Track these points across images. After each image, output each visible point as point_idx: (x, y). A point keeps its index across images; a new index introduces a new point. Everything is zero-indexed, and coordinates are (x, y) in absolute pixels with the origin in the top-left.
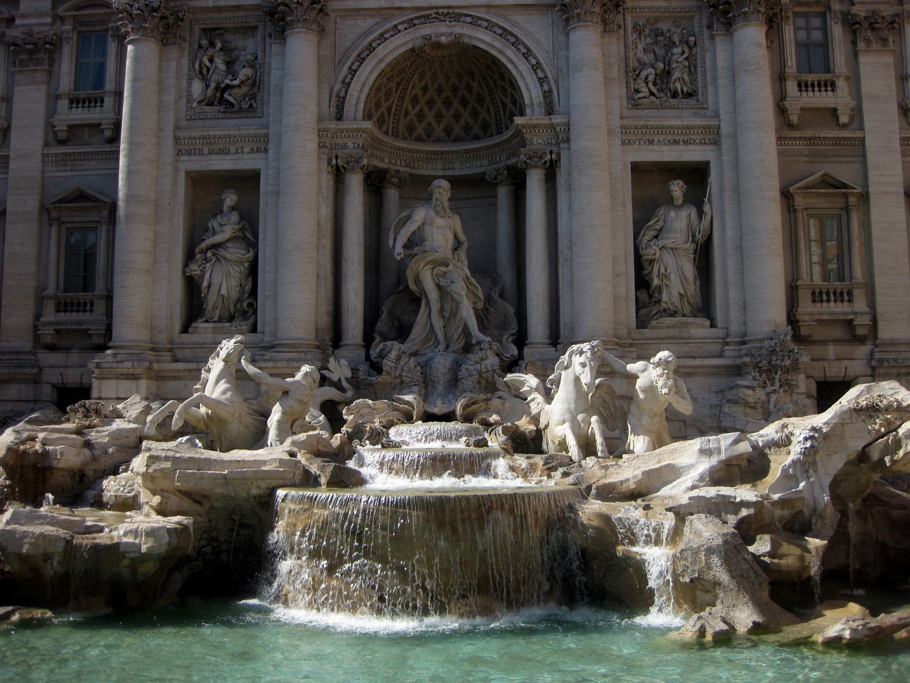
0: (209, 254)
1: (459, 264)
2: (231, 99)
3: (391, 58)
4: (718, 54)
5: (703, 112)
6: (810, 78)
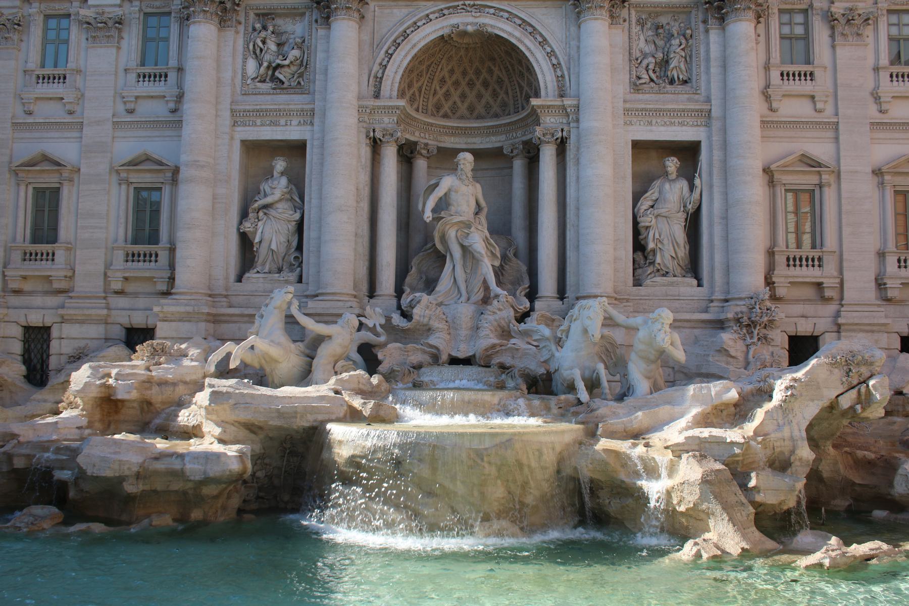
0: (261, 214)
1: (480, 227)
2: (281, 77)
3: (423, 44)
4: (711, 46)
5: (697, 96)
6: (791, 68)
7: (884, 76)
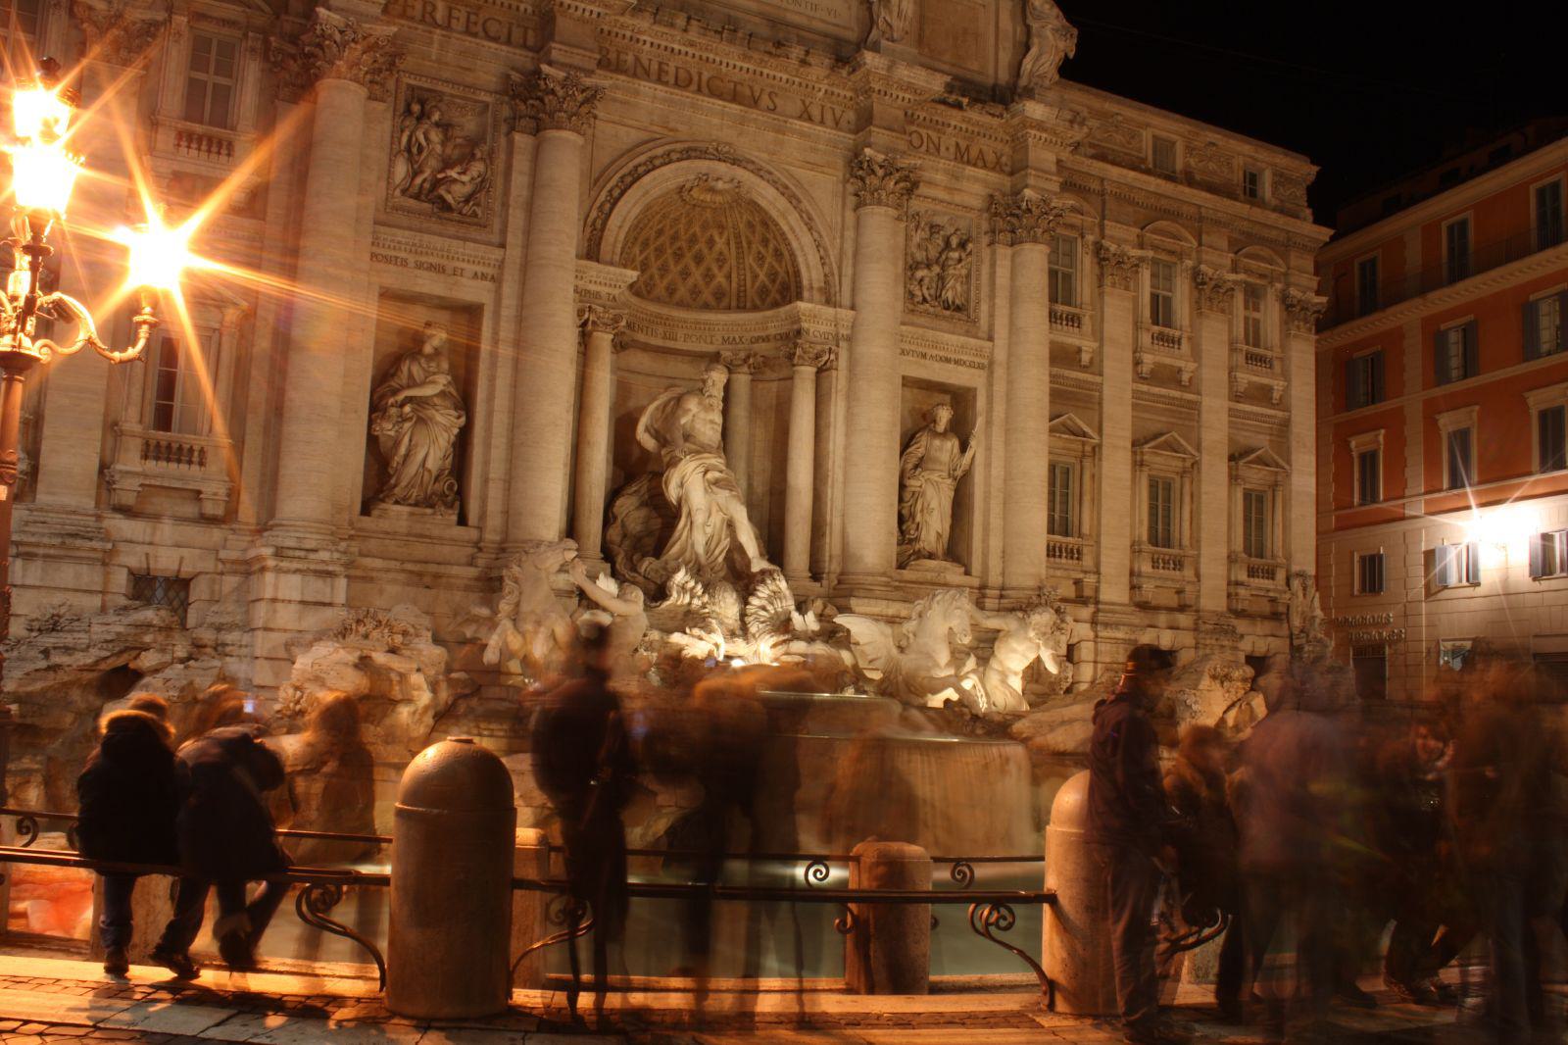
0: (407, 409)
2: (449, 198)
7: (1146, 339)
